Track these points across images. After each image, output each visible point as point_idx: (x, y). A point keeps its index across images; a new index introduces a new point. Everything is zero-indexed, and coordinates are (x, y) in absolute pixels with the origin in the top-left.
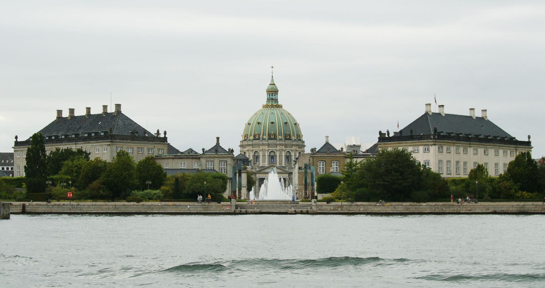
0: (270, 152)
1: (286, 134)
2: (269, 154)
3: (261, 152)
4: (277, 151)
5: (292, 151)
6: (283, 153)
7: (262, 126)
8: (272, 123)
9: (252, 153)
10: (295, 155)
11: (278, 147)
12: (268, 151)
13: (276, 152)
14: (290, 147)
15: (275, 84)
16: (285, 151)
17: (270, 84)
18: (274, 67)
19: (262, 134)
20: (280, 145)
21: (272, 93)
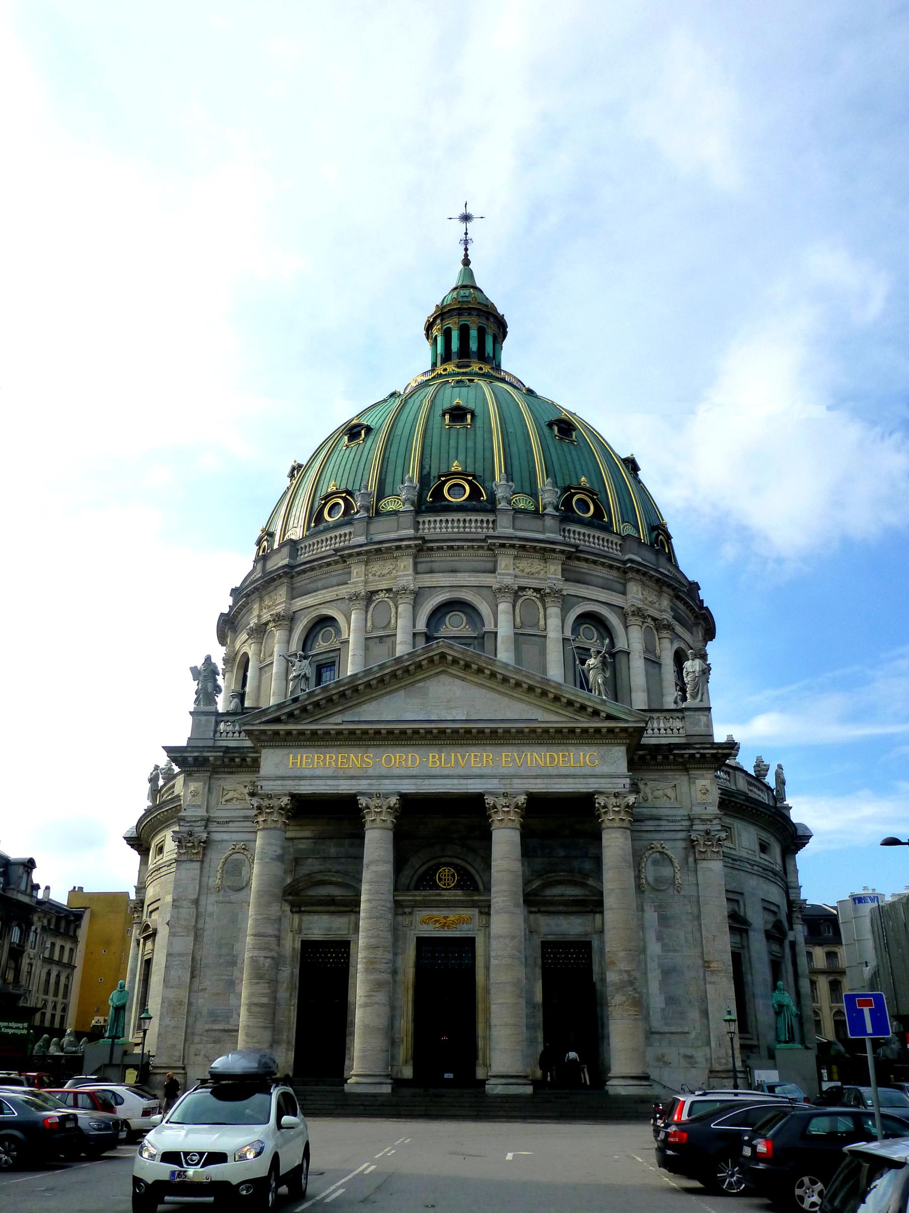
0: (439, 613)
1: (567, 489)
2: (421, 626)
8: (458, 414)
9: (288, 642)
10: (653, 662)
11: (505, 563)
12: (418, 596)
13: (484, 608)
15: (483, 292)
16: (566, 602)
17: (454, 286)
18: (470, 211)
19: (373, 487)
21: (465, 320)
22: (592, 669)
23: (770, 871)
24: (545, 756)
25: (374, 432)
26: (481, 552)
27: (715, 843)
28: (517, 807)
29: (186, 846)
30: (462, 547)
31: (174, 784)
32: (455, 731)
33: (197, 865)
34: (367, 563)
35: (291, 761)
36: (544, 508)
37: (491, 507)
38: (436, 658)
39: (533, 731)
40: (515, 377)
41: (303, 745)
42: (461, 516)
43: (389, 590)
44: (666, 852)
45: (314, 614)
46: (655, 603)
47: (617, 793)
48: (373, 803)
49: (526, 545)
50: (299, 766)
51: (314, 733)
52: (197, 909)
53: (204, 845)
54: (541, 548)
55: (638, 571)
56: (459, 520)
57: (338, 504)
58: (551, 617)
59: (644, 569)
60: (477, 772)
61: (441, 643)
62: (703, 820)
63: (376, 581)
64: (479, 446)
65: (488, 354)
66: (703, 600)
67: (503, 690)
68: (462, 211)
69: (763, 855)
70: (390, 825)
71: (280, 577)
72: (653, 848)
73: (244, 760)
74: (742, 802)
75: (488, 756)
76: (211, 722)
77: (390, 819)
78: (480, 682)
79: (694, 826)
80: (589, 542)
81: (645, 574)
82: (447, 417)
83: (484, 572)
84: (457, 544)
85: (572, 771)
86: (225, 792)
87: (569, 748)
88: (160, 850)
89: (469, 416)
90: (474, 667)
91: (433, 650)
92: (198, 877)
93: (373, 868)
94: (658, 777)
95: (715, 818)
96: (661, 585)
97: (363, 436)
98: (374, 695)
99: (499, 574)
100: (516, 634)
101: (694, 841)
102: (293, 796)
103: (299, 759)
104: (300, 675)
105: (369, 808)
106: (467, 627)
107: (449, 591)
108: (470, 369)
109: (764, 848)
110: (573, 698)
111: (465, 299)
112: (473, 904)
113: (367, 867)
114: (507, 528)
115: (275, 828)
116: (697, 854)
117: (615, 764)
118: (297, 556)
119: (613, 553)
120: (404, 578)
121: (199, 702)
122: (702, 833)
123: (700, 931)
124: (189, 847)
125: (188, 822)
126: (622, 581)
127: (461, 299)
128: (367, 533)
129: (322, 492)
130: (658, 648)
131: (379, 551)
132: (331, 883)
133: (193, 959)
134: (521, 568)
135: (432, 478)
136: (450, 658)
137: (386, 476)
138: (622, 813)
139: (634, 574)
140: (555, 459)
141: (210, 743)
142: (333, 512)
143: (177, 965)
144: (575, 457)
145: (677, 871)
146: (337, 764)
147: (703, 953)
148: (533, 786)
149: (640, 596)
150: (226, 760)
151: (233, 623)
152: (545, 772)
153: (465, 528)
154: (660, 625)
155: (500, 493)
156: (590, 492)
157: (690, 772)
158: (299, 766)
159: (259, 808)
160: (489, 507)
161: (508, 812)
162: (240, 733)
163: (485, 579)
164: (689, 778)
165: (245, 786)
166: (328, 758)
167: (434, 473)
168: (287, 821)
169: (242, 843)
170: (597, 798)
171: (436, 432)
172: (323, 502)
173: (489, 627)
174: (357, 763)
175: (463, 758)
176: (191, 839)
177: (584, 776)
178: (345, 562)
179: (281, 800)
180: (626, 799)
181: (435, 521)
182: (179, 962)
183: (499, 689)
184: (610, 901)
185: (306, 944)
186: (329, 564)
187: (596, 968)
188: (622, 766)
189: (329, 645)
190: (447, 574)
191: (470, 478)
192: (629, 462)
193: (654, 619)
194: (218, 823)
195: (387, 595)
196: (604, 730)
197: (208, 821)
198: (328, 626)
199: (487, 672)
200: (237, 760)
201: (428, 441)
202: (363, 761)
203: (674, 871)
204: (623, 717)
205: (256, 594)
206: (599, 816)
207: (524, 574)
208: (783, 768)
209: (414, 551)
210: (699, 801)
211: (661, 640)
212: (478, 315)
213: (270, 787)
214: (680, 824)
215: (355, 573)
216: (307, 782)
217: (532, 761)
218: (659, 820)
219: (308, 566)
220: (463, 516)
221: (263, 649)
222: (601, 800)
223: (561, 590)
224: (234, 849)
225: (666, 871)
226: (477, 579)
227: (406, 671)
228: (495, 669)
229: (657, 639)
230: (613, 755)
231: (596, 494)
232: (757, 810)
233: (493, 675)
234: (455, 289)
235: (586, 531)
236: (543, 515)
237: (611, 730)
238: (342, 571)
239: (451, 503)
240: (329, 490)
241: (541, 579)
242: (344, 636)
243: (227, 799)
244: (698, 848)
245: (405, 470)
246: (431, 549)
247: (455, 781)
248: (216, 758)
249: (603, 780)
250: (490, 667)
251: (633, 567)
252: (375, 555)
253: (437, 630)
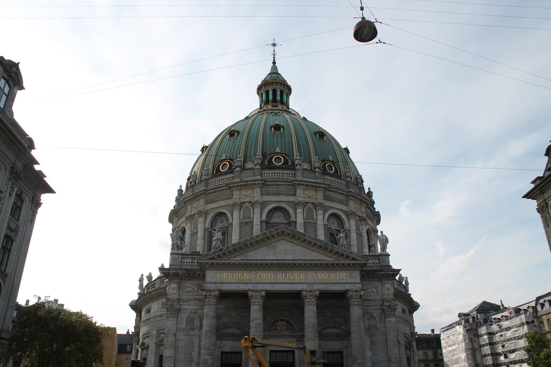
1: (323, 161)
2: (264, 217)
3: (236, 213)
4: (295, 205)
5: (347, 214)
6: (320, 217)
7: (242, 138)
8: (277, 127)
9: (205, 223)
10: (359, 235)
11: (299, 192)
12: (263, 205)
13: (291, 211)
14: (340, 202)
15: (281, 75)
16: (325, 209)
17: (269, 72)
20: (308, 186)
21: (274, 87)
22: (341, 238)
23: (406, 321)
24: (327, 275)
25: (241, 134)
26: (289, 187)
27: (392, 310)
28: (315, 296)
29: (170, 311)
30: (282, 184)
31: (155, 283)
32: (289, 264)
33: (175, 319)
34: (240, 190)
35: (219, 276)
36: (315, 168)
37: (293, 167)
38: (280, 233)
39: (322, 264)
40: (296, 112)
41: (223, 269)
42: (281, 171)
43: (250, 202)
44: (373, 314)
45: (216, 211)
46: (359, 209)
47: (357, 290)
48: (254, 294)
49: (308, 184)
50: (222, 278)
51: (229, 264)
52: (176, 337)
53: (178, 311)
54: (315, 186)
55: (353, 196)
56: (279, 173)
57: (226, 164)
58: (319, 215)
59: (356, 195)
60: (298, 281)
61: (283, 227)
62: (388, 301)
63: (244, 198)
64: (287, 141)
65: (284, 102)
66: (375, 208)
67: (308, 247)
68: (273, 42)
69: (403, 315)
70: (261, 303)
71: (201, 194)
72: (367, 313)
73: (194, 274)
74: (397, 293)
75: (302, 275)
76: (180, 258)
77: (261, 301)
78: (298, 243)
79: (384, 304)
80: (333, 183)
81: (356, 197)
82: (273, 129)
83: (291, 195)
84: (279, 183)
85: (338, 281)
86: (186, 288)
87: (337, 272)
88: (149, 311)
89: (282, 129)
90: (297, 237)
91: (279, 230)
92: (176, 324)
93: (255, 322)
94: (369, 283)
95: (393, 300)
96: (362, 202)
97: (236, 135)
98: (254, 248)
99: (297, 196)
100: (304, 222)
101: (384, 310)
102: (220, 291)
103: (222, 275)
104: (218, 239)
105: (252, 296)
106: (283, 219)
107: (276, 203)
108: (278, 108)
109: (404, 312)
110: (338, 251)
111: (275, 78)
112: (294, 337)
113: (253, 321)
114: (301, 177)
115: (213, 304)
116: (385, 315)
117: (355, 279)
118: (208, 186)
119: (343, 188)
120: (257, 197)
121: (174, 248)
122: (388, 306)
123: (387, 346)
124: (172, 311)
125: (171, 300)
126: (347, 200)
127: (273, 78)
128: (240, 178)
130: (361, 228)
131: (246, 185)
132: (233, 328)
133: (175, 358)
134: (306, 194)
135: (267, 154)
136: (286, 233)
137: (247, 153)
138: (359, 298)
139: (352, 197)
140: (318, 148)
141: (180, 267)
142: (224, 167)
143: (168, 361)
144: (326, 147)
145: (377, 322)
146: (238, 278)
147: (388, 355)
148: (322, 288)
149: (354, 207)
150: (187, 274)
151: (177, 214)
152: (326, 282)
153: (282, 176)
154: (362, 219)
155: (297, 162)
156: (333, 162)
157: (383, 281)
158: (222, 278)
159: (205, 296)
160: (292, 167)
161: (312, 298)
162: (192, 263)
163: (291, 198)
164: (382, 284)
165: (195, 286)
166: (234, 275)
167: (268, 152)
168: (217, 302)
169: (194, 310)
170: (349, 293)
171: (268, 135)
172: (219, 163)
173: (293, 219)
174: (247, 277)
175: (292, 276)
176: (172, 308)
177: (343, 283)
178: (230, 189)
179: (215, 292)
180: (360, 293)
181: (270, 173)
182: (168, 360)
183: (306, 246)
184: (353, 335)
185: (222, 353)
186: (223, 190)
187: (345, 362)
188: (358, 280)
189: (223, 225)
190: (274, 196)
191: (284, 155)
192: (346, 150)
193: (359, 216)
194: (184, 301)
195: (249, 204)
196: (351, 264)
197: (179, 300)
198: (222, 217)
199: (302, 239)
200: (192, 274)
201: (265, 139)
202: (249, 276)
203: (376, 322)
204: (359, 259)
205: (190, 202)
206: (349, 300)
207: (307, 197)
208: (408, 278)
209: (261, 186)
210: (386, 293)
211: (363, 225)
212: (280, 85)
213: (210, 287)
214: (378, 303)
215: (235, 194)
216: (226, 285)
217: (321, 277)
218: (370, 301)
219: (214, 190)
220: (281, 171)
221: (193, 226)
222: (350, 293)
223: (323, 204)
224: (190, 312)
225: (373, 322)
226: (288, 198)
227: (268, 238)
228: (306, 238)
229: (360, 225)
230: (355, 275)
231: (334, 163)
232: (402, 296)
233: (305, 240)
234: (270, 74)
235: (332, 179)
236: (315, 172)
237: (354, 264)
238: (228, 193)
239: (276, 166)
240: (222, 158)
241: (314, 199)
242: (230, 221)
243: (187, 291)
244: (385, 312)
245: (256, 151)
246: (268, 185)
247: (289, 285)
248: (183, 274)
249: (351, 285)
250: (303, 237)
251: (351, 194)
252: (244, 187)
253: (270, 219)
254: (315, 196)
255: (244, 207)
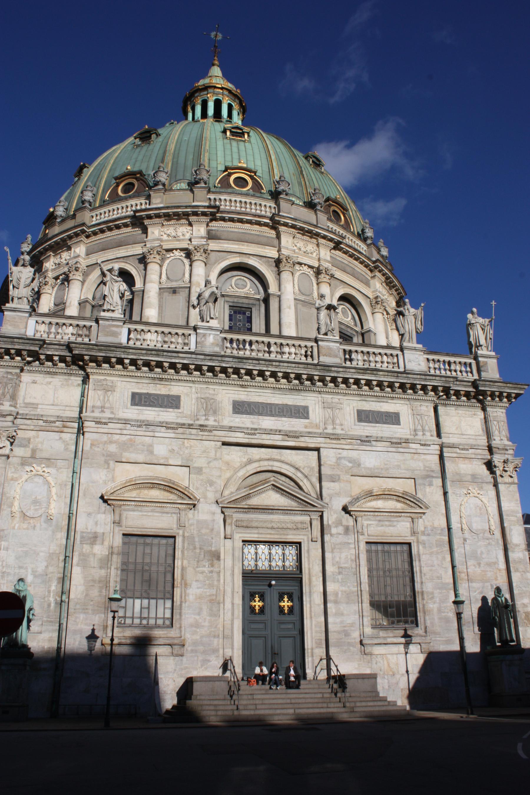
13: (269, 275)
55: (380, 271)
57: (132, 185)
71: (77, 235)
82: (228, 133)
89: (246, 136)
107: (239, 256)
118: (92, 221)
129: (117, 174)
191: (253, 174)
242: (139, 284)
254: (315, 254)
255: (170, 259)
